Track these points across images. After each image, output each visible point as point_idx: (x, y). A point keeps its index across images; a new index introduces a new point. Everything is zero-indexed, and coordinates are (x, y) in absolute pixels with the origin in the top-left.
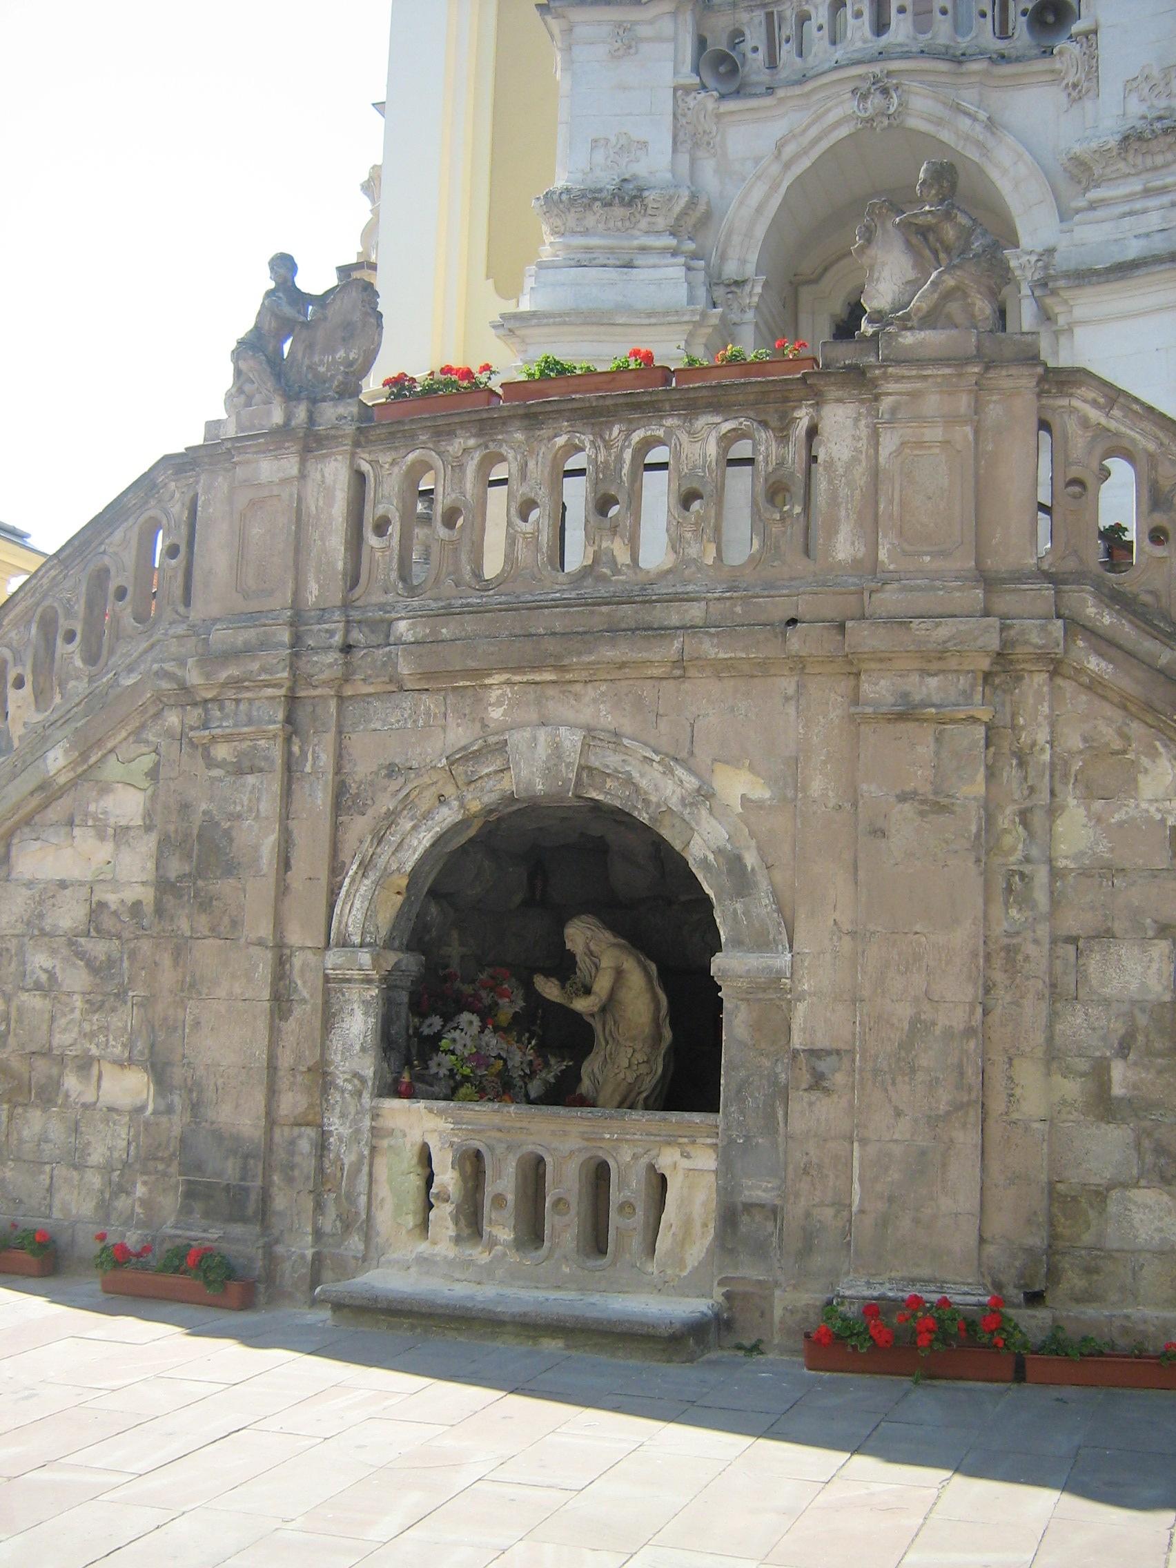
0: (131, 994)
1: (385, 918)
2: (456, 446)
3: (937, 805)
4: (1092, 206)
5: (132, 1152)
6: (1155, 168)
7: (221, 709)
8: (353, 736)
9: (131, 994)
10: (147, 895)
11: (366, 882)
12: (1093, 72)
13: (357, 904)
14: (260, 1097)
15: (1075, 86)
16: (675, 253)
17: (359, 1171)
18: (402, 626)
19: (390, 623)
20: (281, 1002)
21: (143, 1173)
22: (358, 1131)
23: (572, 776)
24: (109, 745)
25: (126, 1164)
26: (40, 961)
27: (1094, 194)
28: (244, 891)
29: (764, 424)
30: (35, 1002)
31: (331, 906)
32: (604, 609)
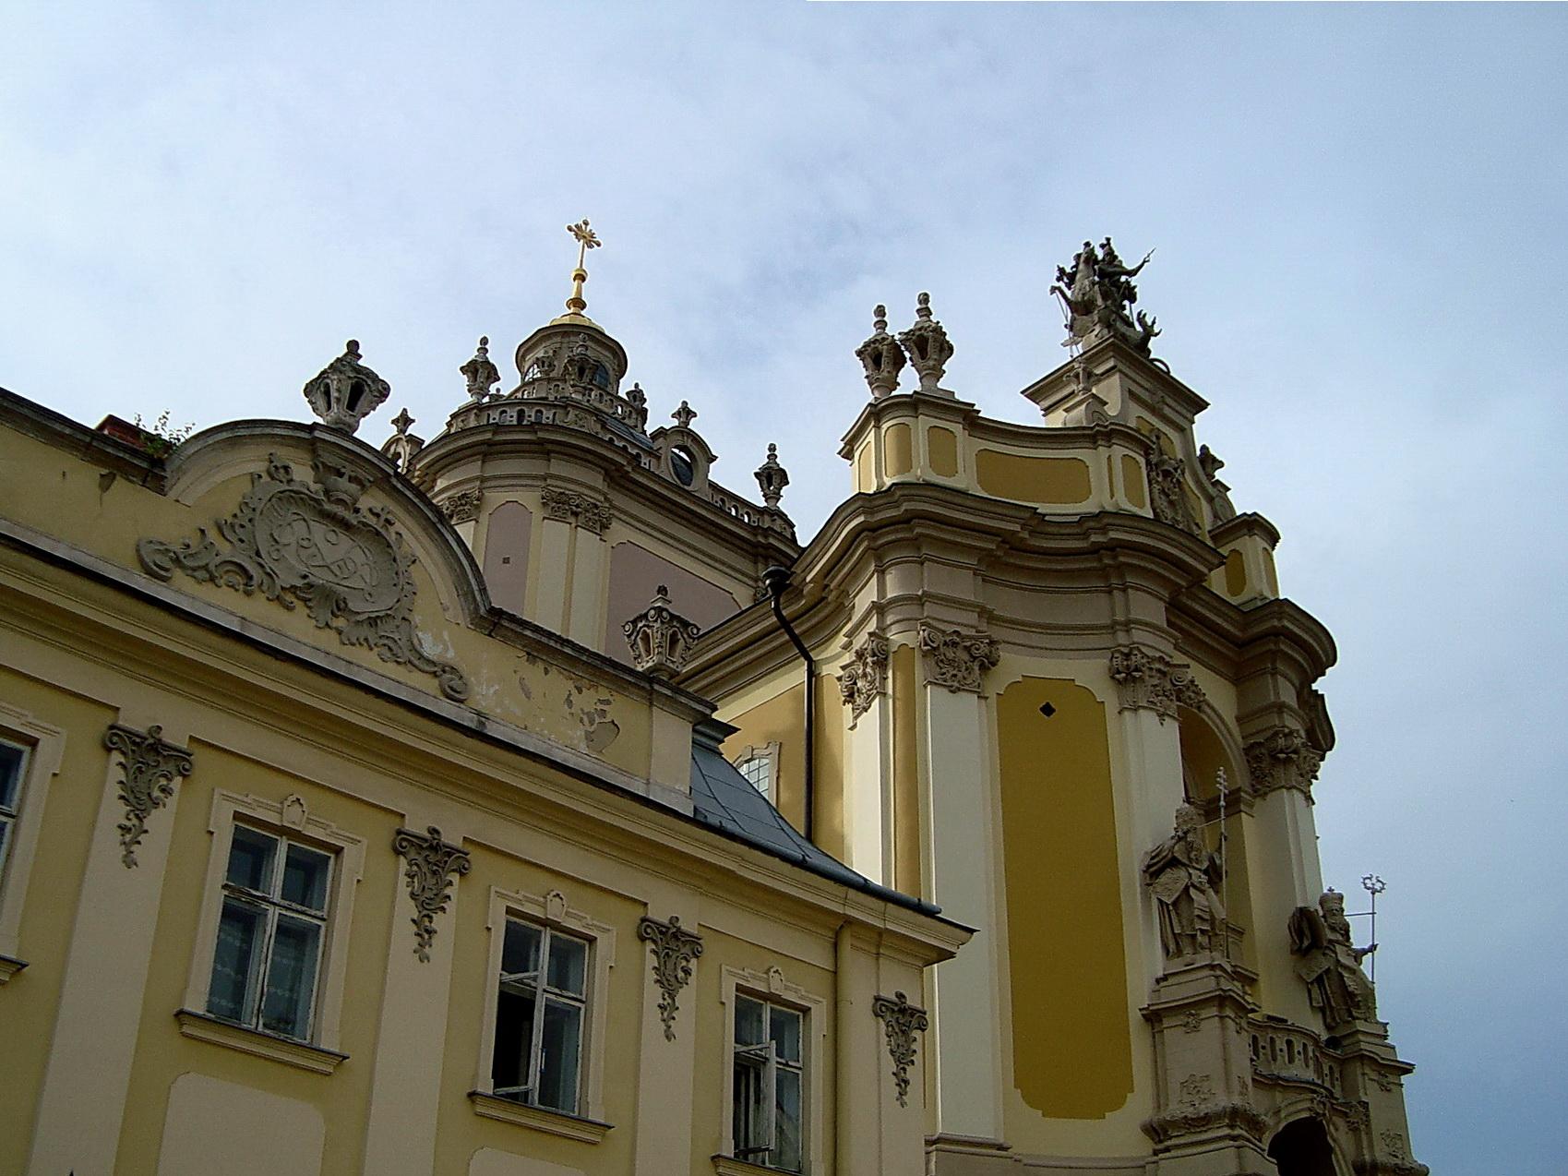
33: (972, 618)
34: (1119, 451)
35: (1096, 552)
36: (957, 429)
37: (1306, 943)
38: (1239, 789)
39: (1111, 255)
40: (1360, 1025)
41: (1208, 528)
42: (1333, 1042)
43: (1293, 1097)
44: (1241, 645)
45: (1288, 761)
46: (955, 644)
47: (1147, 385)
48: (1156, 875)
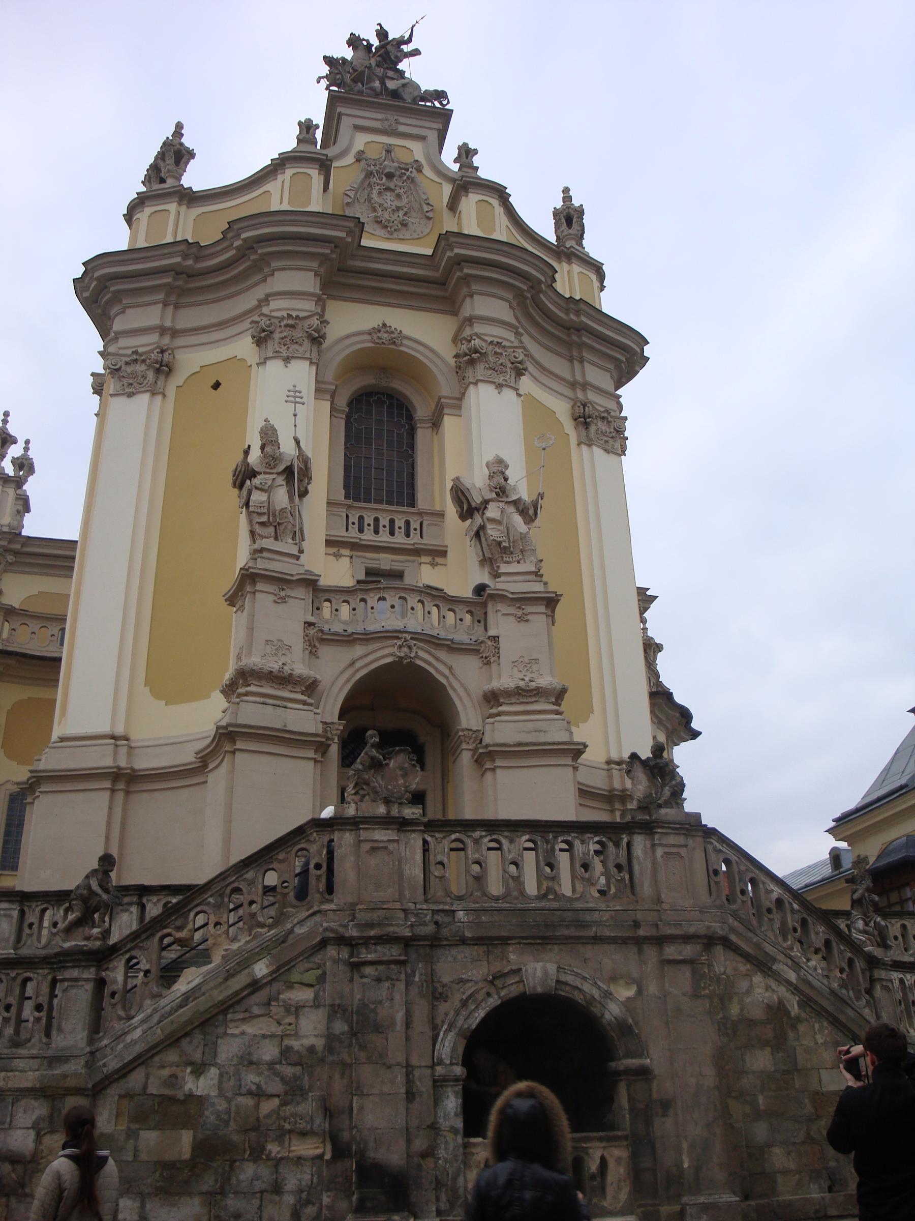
0: (310, 1094)
1: (460, 1050)
2: (477, 834)
3: (696, 995)
4: (499, 714)
5: (315, 1180)
6: (527, 703)
7: (367, 948)
8: (438, 964)
9: (310, 1094)
10: (319, 1043)
11: (452, 1034)
12: (497, 654)
13: (447, 1044)
14: (402, 1143)
15: (486, 658)
16: (305, 703)
17: (459, 1175)
18: (461, 914)
19: (454, 912)
20: (410, 1095)
21: (327, 1191)
22: (456, 1156)
23: (554, 985)
24: (292, 964)
25: (310, 1187)
26: (251, 1079)
27: (501, 709)
28: (387, 1040)
29: (610, 839)
30: (249, 1101)
31: (434, 1045)
32: (558, 913)
33: (153, 338)
34: (289, 172)
35: (245, 255)
36: (172, 207)
37: (465, 508)
38: (440, 398)
39: (382, 34)
40: (504, 568)
41: (445, 203)
42: (480, 589)
43: (371, 647)
44: (442, 283)
45: (472, 362)
46: (136, 361)
47: (380, 116)
48: (241, 487)
